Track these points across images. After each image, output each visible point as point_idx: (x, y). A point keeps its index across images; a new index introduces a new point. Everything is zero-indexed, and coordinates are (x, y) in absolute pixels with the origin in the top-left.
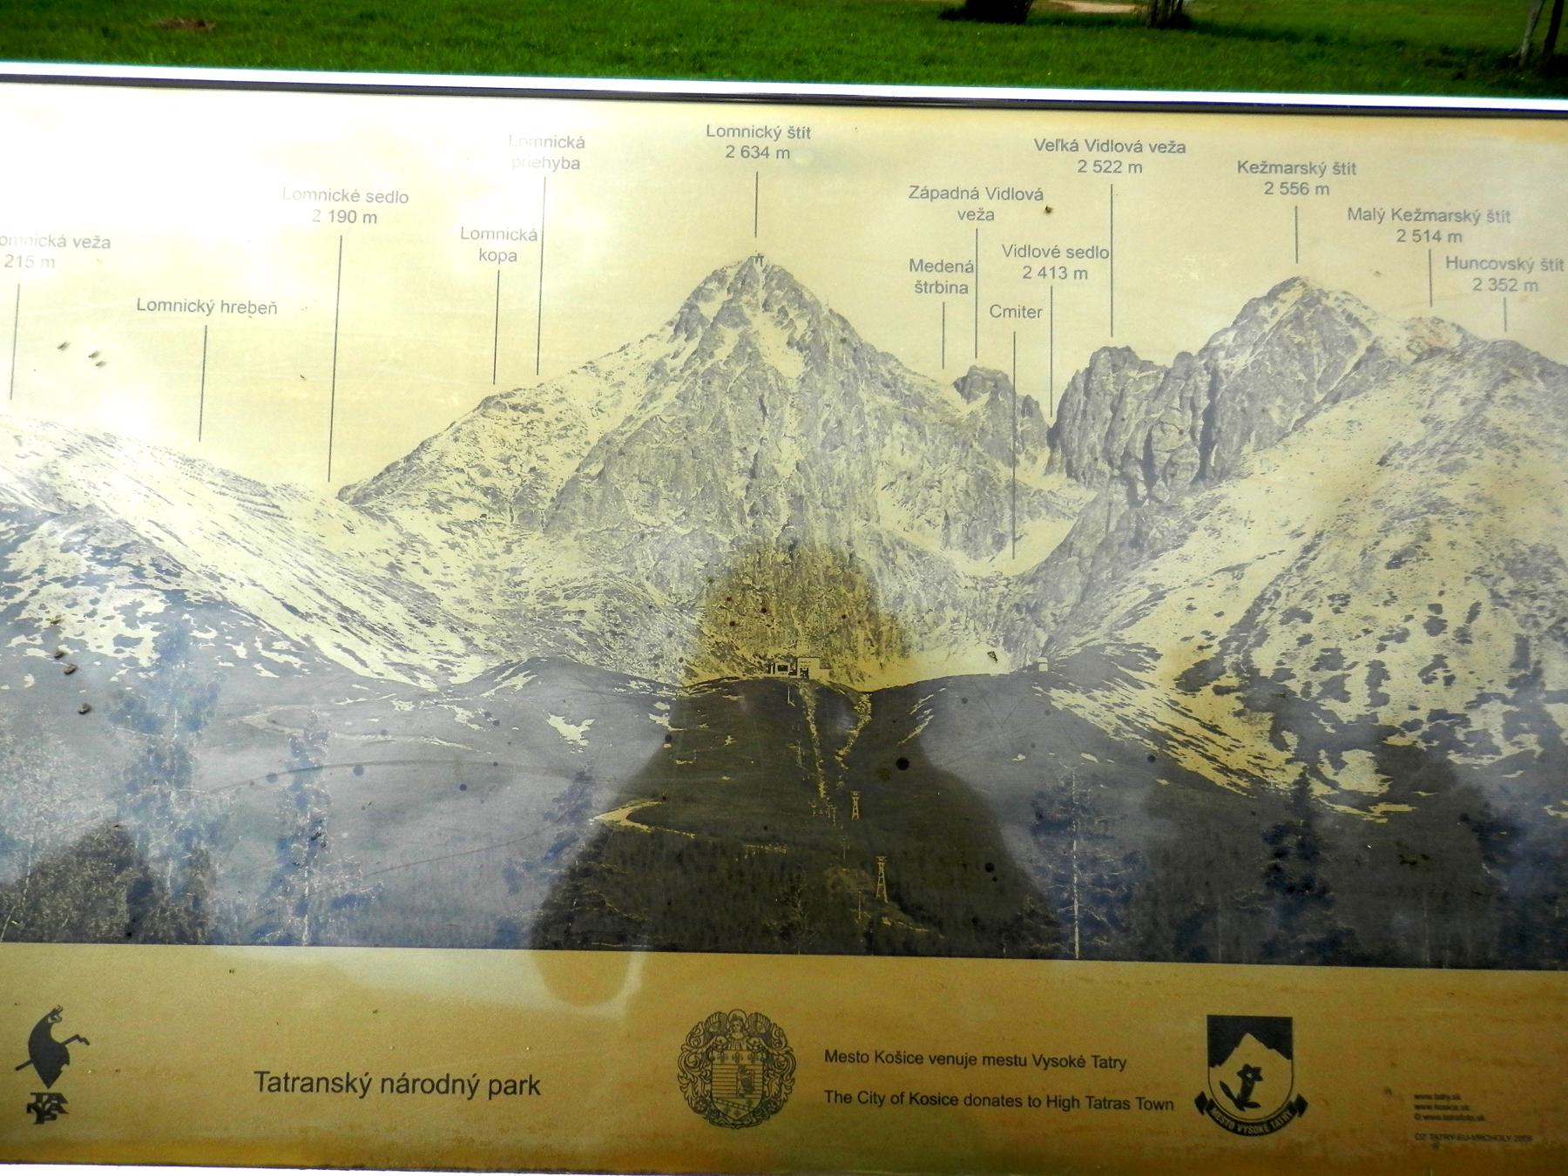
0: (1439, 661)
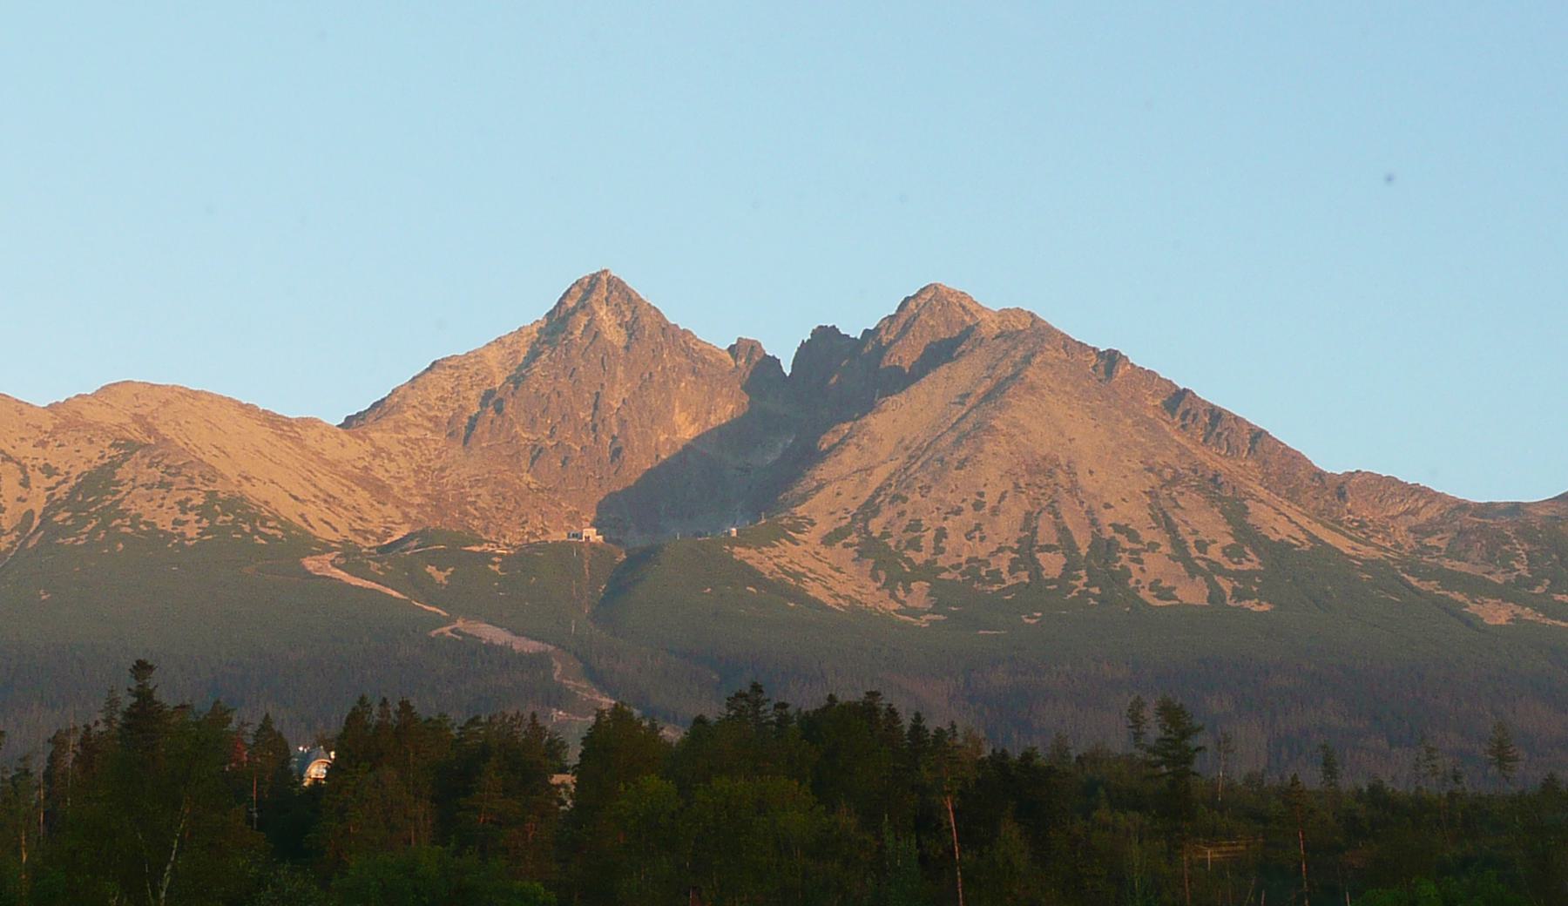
0: (978, 527)
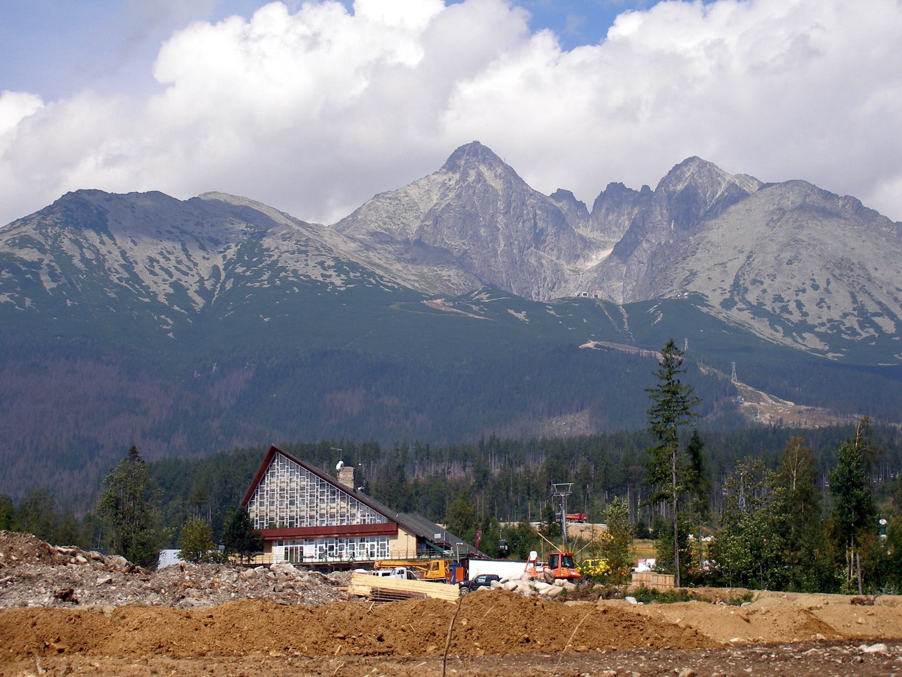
0: (822, 300)
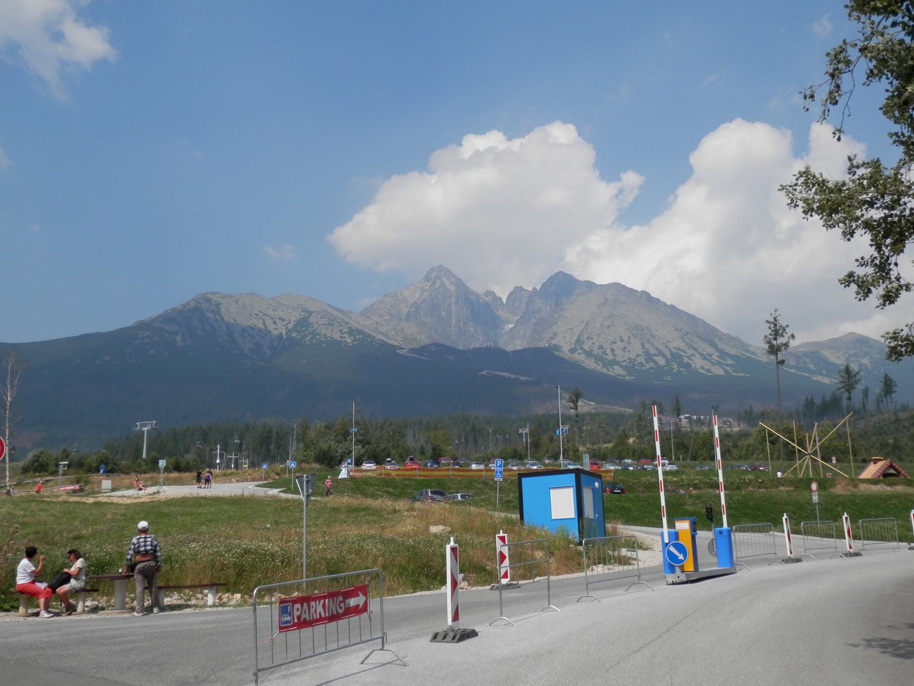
0: (625, 348)
